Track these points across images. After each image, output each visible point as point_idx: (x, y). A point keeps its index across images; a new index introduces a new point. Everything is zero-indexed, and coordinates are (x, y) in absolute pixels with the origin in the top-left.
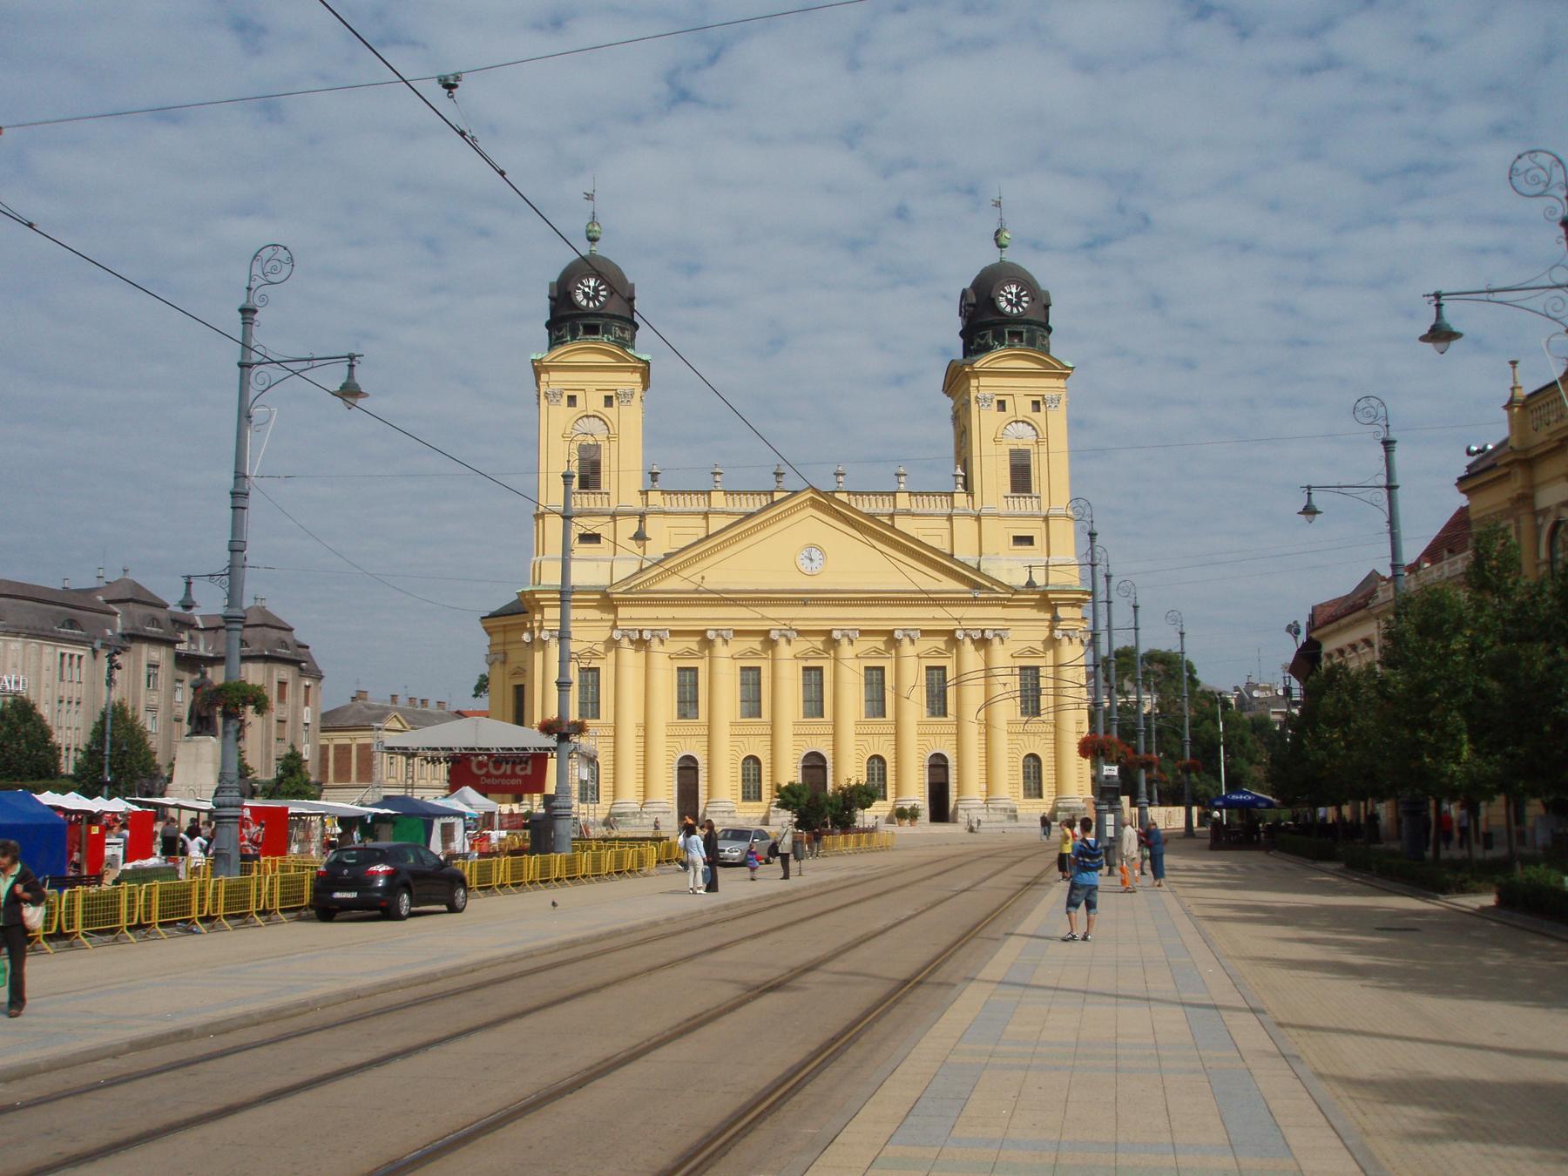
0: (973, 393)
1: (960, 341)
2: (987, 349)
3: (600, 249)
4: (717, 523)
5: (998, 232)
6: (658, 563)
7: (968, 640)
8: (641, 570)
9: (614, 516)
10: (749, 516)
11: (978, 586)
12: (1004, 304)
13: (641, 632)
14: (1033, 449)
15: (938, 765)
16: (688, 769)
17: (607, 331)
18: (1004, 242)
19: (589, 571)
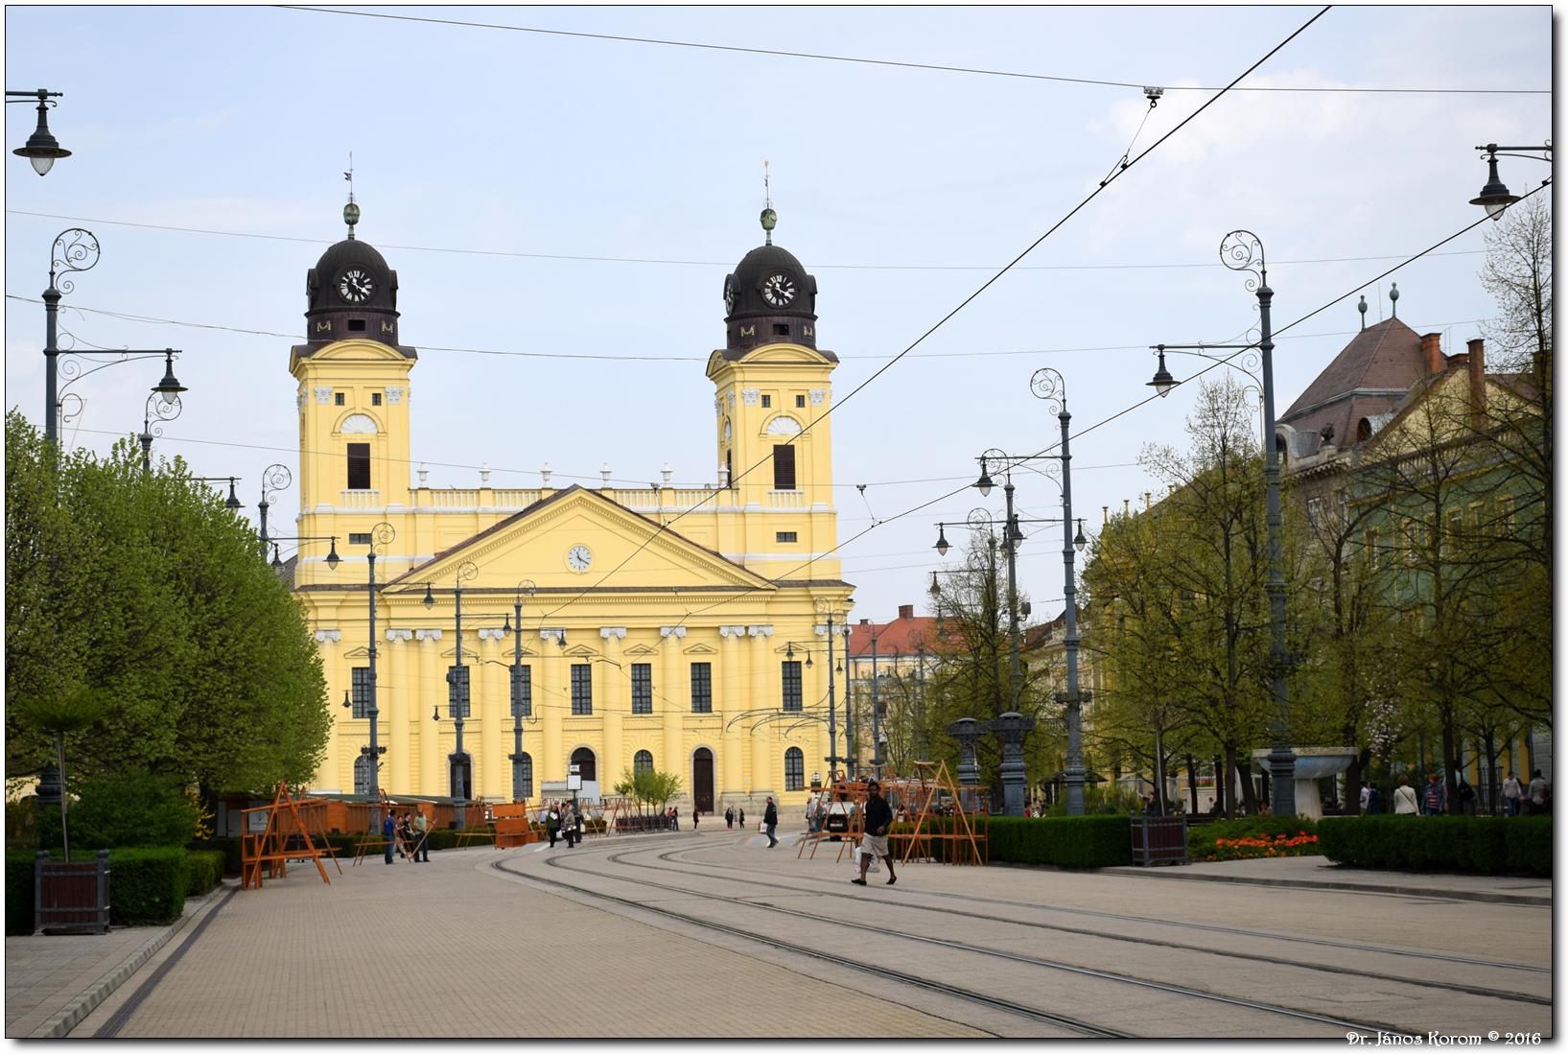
0: (739, 387)
1: (725, 327)
3: (362, 234)
5: (765, 214)
6: (431, 563)
7: (732, 637)
11: (746, 587)
12: (769, 296)
14: (798, 445)
15: (703, 761)
16: (460, 764)
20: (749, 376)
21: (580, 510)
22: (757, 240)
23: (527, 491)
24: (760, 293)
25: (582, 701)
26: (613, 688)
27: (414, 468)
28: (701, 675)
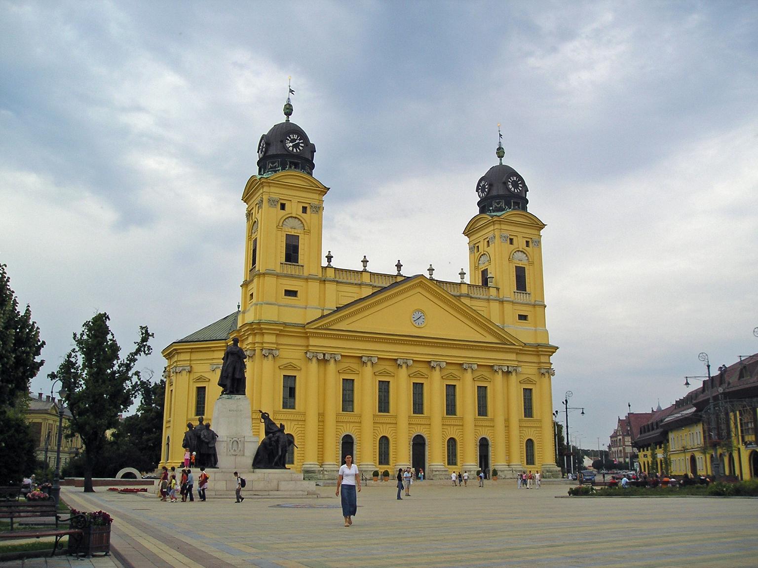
2: (501, 209)
3: (293, 119)
4: (368, 291)
6: (335, 312)
7: (500, 372)
8: (323, 317)
9: (307, 279)
10: (384, 289)
13: (324, 354)
15: (484, 445)
17: (303, 168)
18: (501, 154)
19: (294, 314)
20: (503, 227)
21: (419, 290)
22: (496, 162)
23: (389, 276)
24: (505, 183)
25: (418, 407)
26: (435, 399)
27: (324, 254)
28: (482, 393)
